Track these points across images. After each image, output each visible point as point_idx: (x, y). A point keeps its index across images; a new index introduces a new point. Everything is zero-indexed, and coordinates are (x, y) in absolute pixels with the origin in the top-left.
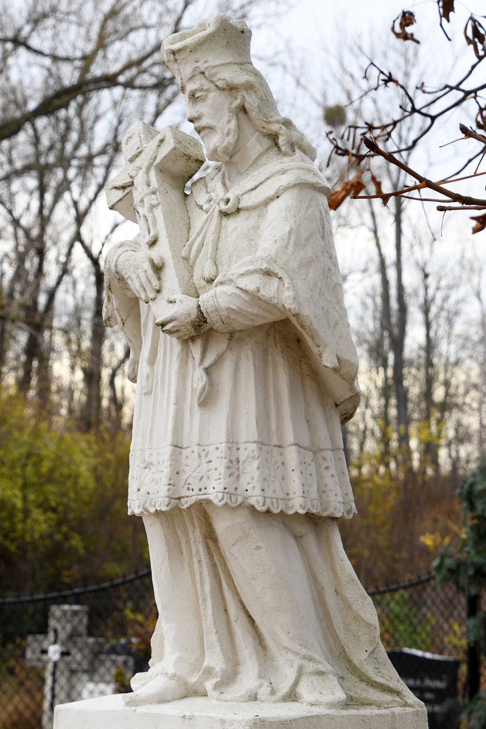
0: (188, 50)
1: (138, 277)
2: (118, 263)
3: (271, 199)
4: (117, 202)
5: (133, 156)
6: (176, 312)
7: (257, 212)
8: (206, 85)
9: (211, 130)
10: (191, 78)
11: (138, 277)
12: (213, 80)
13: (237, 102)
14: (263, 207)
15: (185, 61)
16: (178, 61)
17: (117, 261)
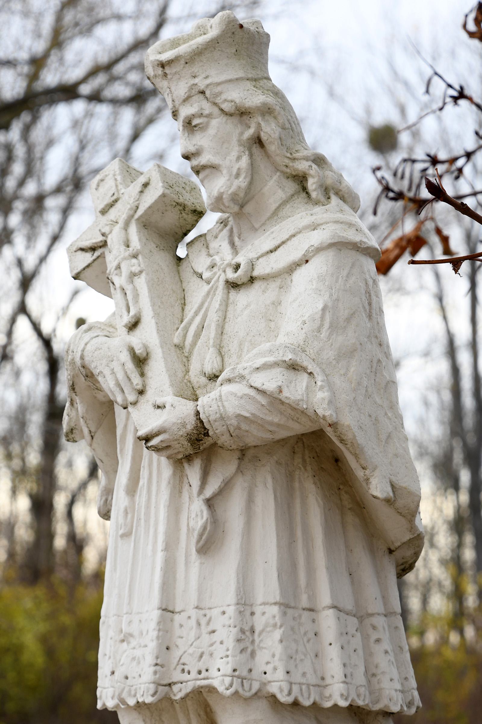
0: (183, 62)
1: (113, 373)
2: (85, 354)
3: (297, 265)
4: (84, 269)
5: (107, 205)
6: (165, 421)
7: (278, 282)
8: (207, 108)
9: (214, 170)
10: (187, 99)
11: (113, 373)
12: (217, 101)
13: (251, 132)
14: (286, 276)
15: (177, 76)
16: (169, 77)
17: (83, 351)
